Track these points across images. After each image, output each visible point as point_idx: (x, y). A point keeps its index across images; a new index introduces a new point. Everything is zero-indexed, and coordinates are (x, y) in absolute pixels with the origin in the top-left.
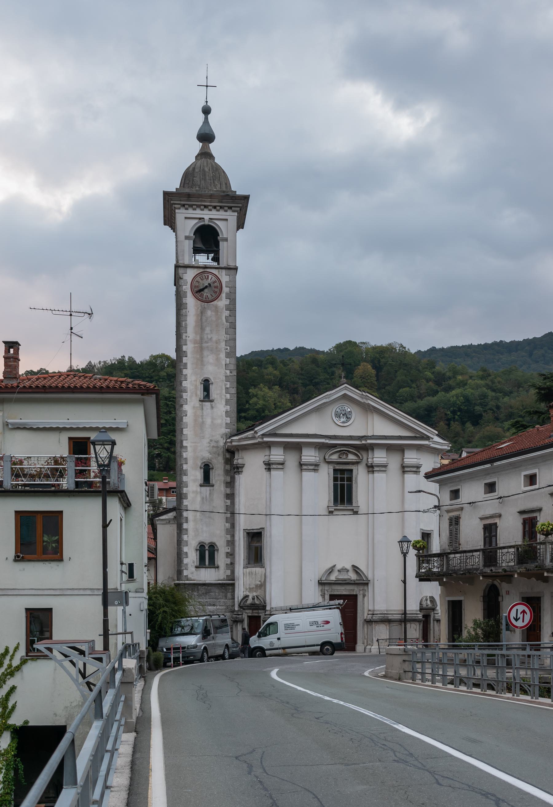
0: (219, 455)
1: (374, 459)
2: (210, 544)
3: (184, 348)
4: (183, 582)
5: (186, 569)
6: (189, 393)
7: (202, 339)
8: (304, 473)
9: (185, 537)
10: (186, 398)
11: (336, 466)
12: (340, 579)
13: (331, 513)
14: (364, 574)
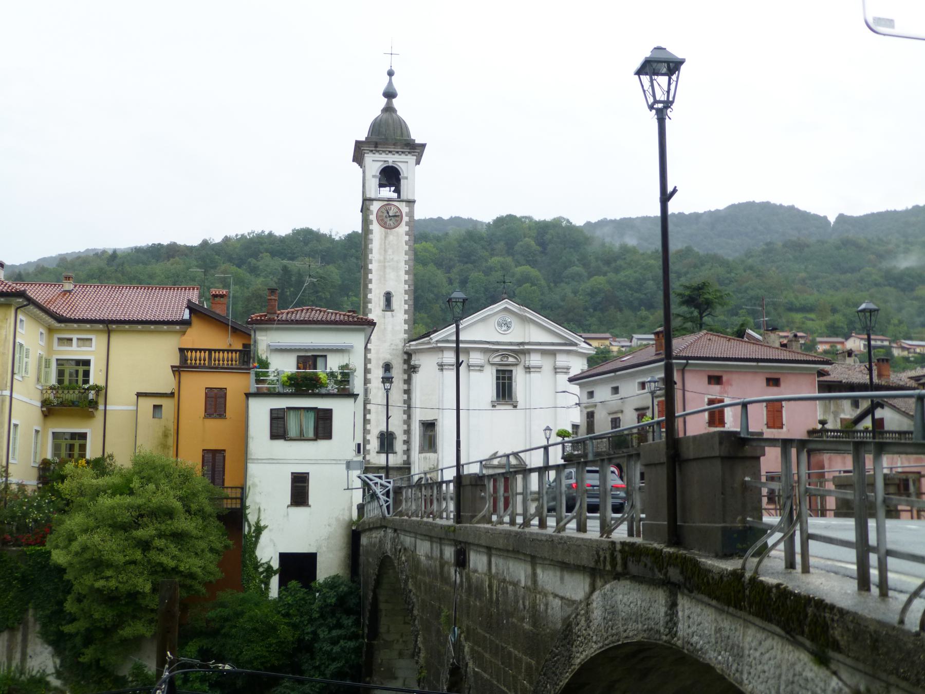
0: (398, 356)
7: (385, 259)
8: (472, 373)
13: (494, 406)
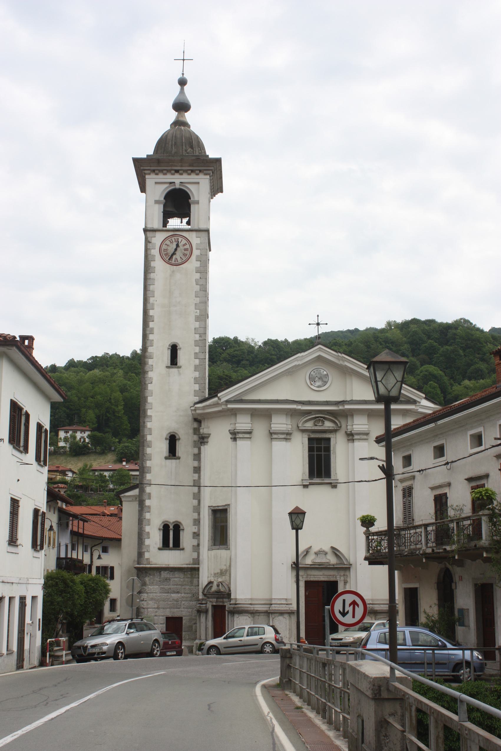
1: (354, 426)
2: (175, 523)
3: (151, 313)
4: (144, 566)
5: (148, 551)
6: (155, 359)
9: (147, 516)
10: (152, 364)
11: (311, 434)
12: (316, 563)
13: (305, 486)
14: (344, 557)
